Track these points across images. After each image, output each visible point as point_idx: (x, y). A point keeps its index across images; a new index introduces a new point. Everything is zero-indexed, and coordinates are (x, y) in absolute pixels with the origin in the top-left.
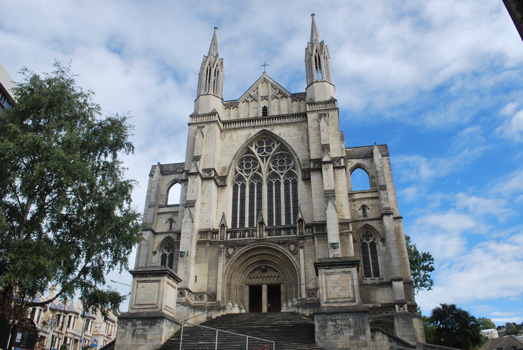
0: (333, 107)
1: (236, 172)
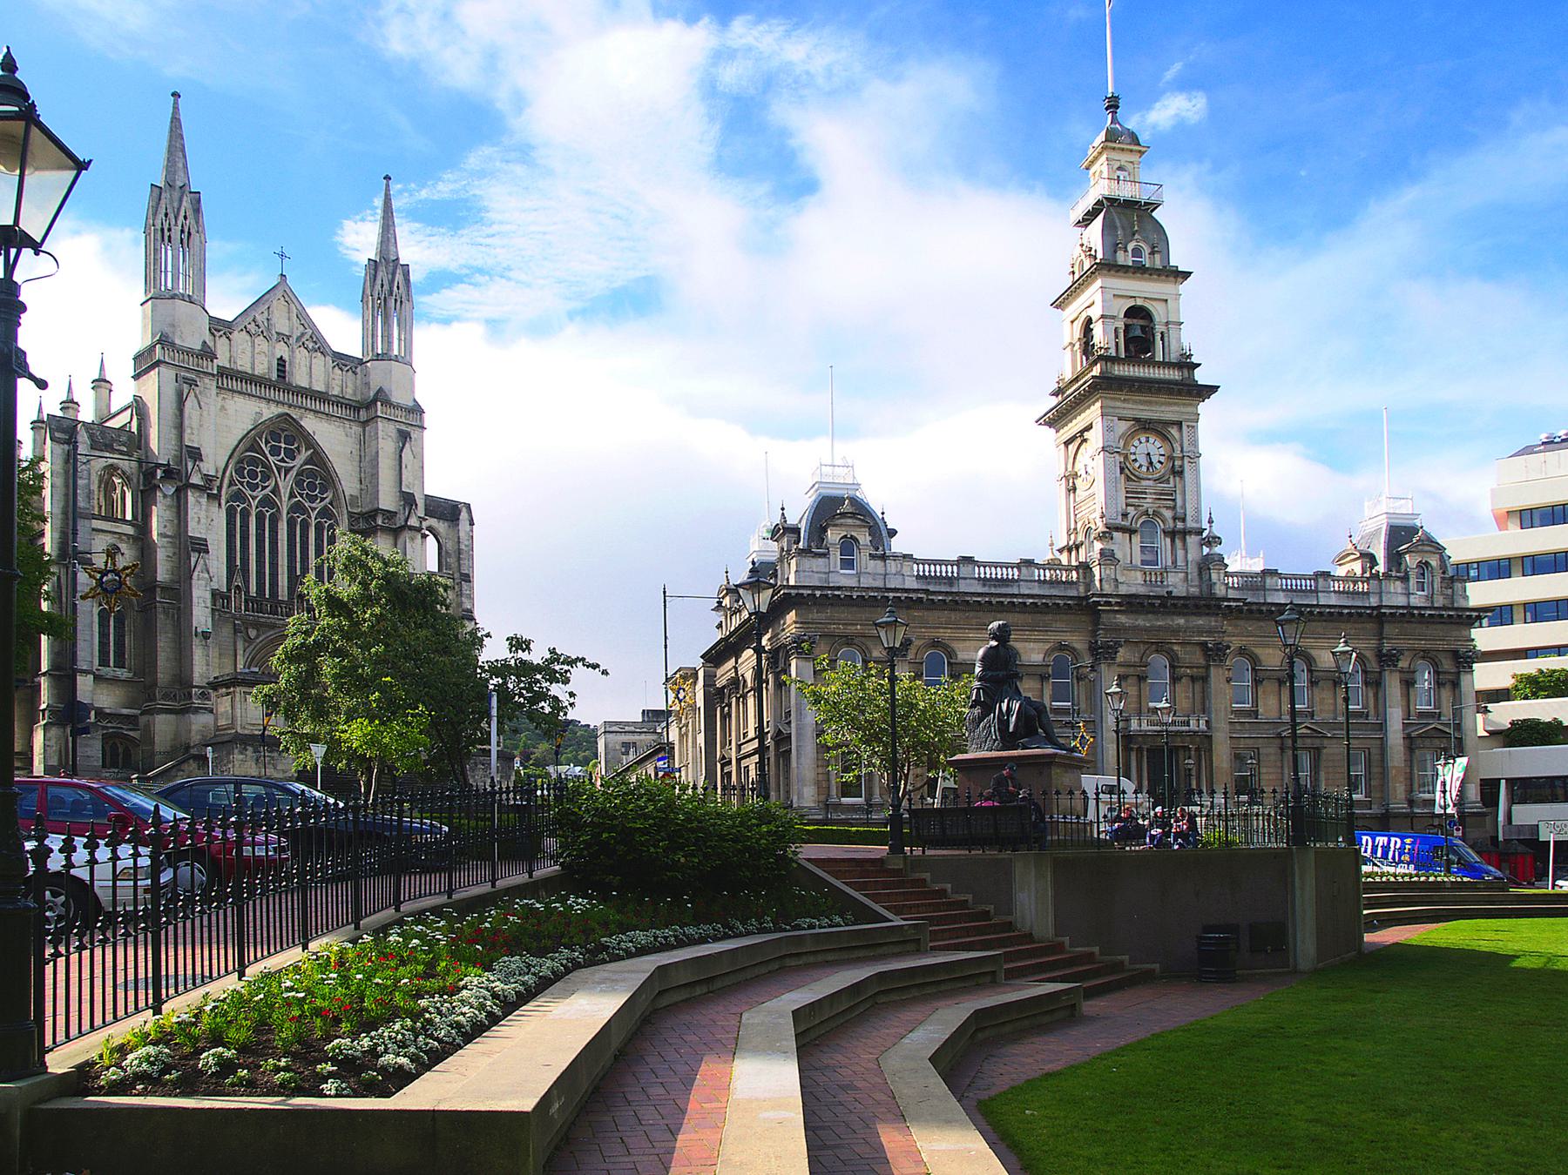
0: (418, 423)
1: (231, 484)
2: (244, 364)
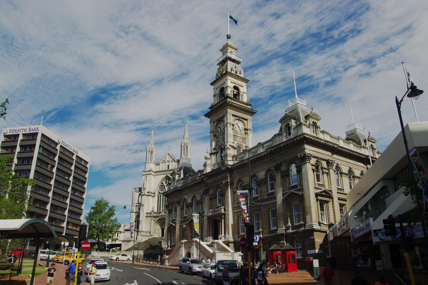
2: (161, 169)
